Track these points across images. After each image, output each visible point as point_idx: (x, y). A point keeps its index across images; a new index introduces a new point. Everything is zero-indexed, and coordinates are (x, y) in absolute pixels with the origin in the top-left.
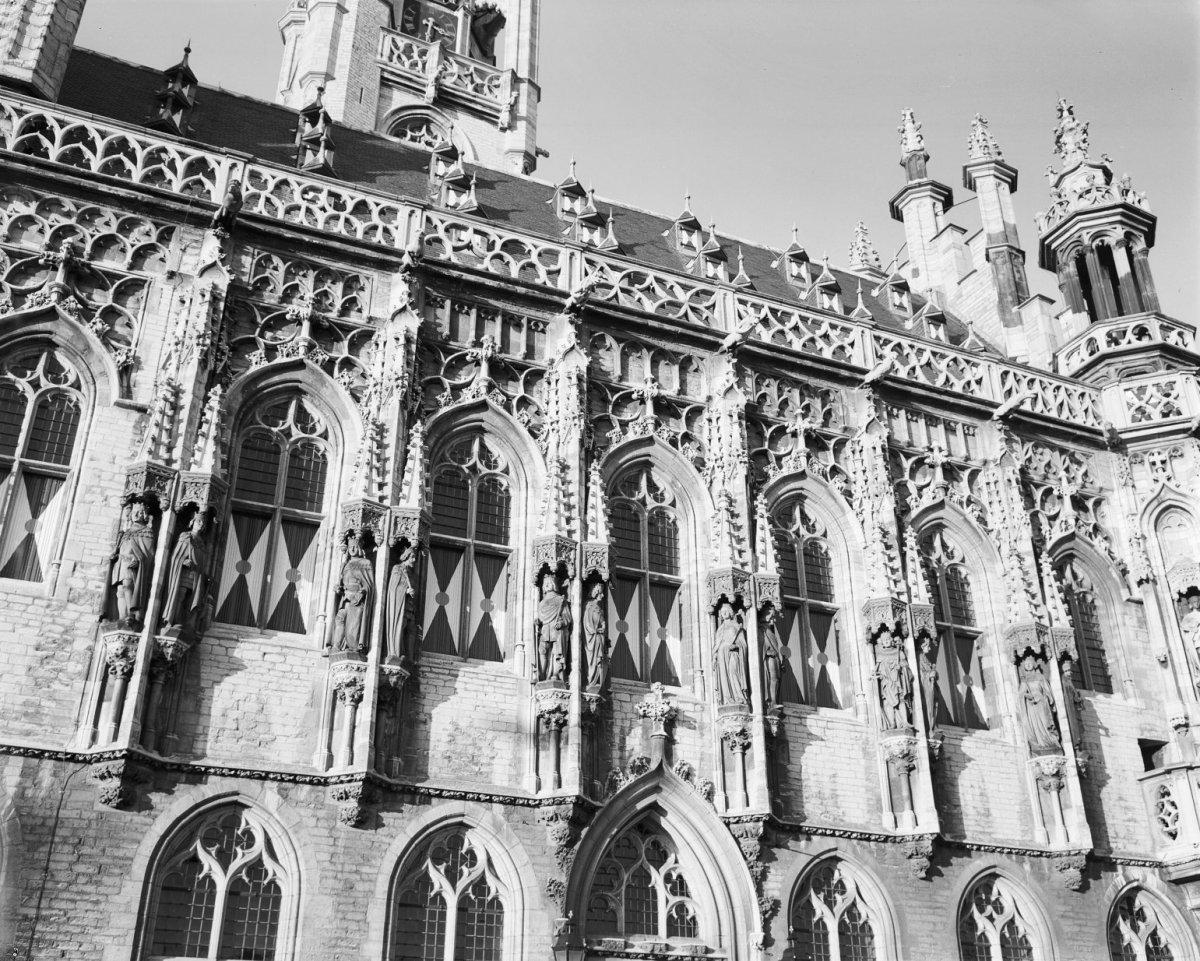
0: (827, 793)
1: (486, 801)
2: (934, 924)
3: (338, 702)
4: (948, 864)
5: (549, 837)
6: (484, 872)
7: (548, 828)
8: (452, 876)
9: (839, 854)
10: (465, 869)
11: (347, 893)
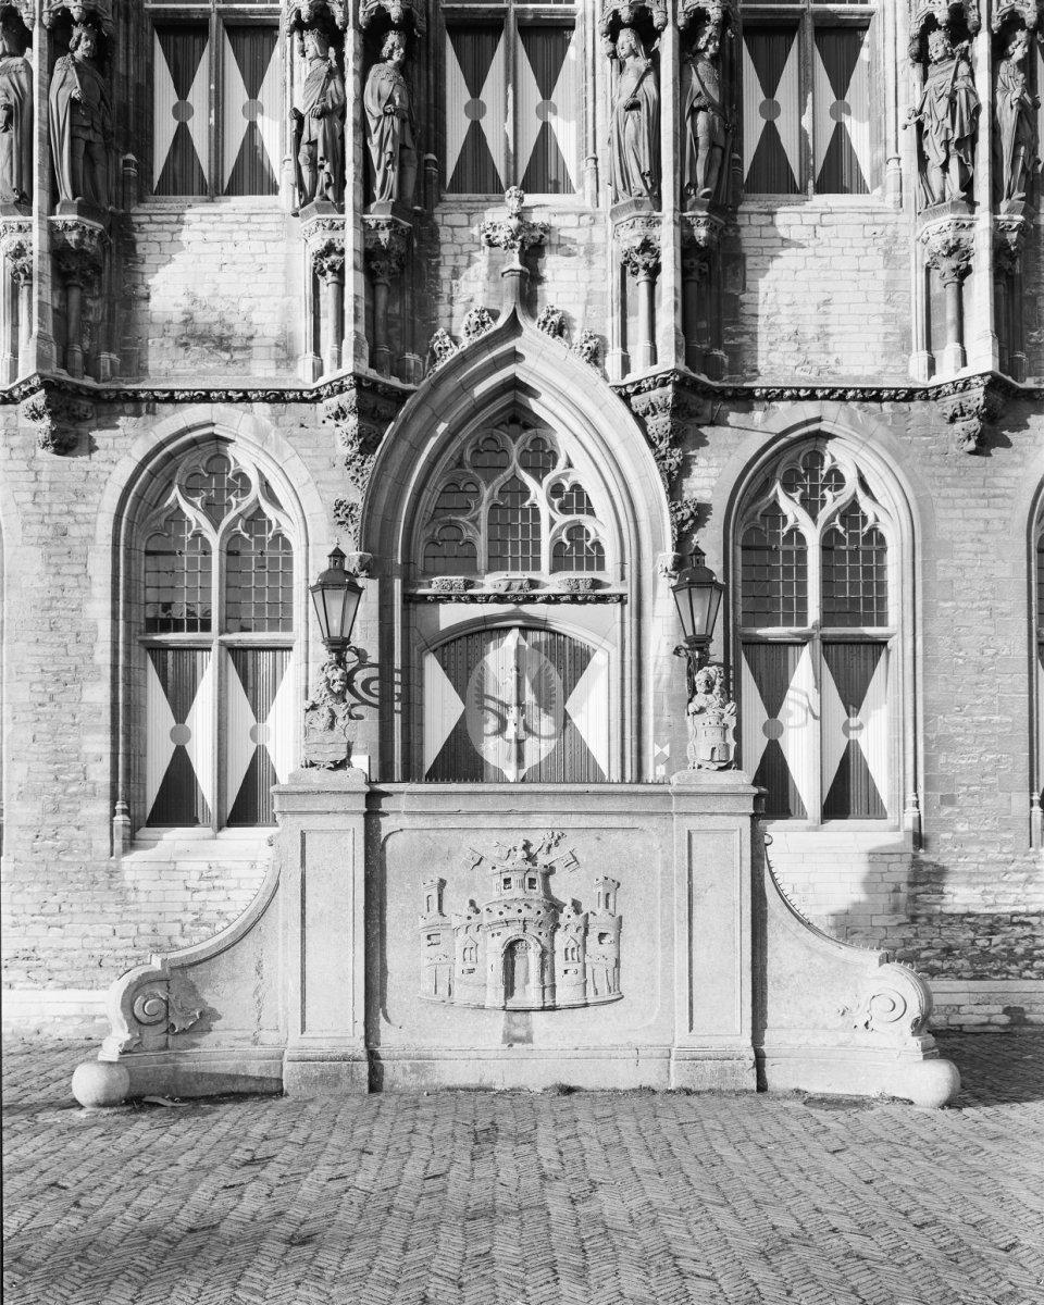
0: (810, 331)
1: (240, 400)
2: (987, 522)
3: (629, 278)
4: (1021, 426)
5: (340, 443)
6: (855, 495)
7: (338, 430)
8: (811, 506)
9: (825, 427)
10: (828, 494)
11: (58, 540)
